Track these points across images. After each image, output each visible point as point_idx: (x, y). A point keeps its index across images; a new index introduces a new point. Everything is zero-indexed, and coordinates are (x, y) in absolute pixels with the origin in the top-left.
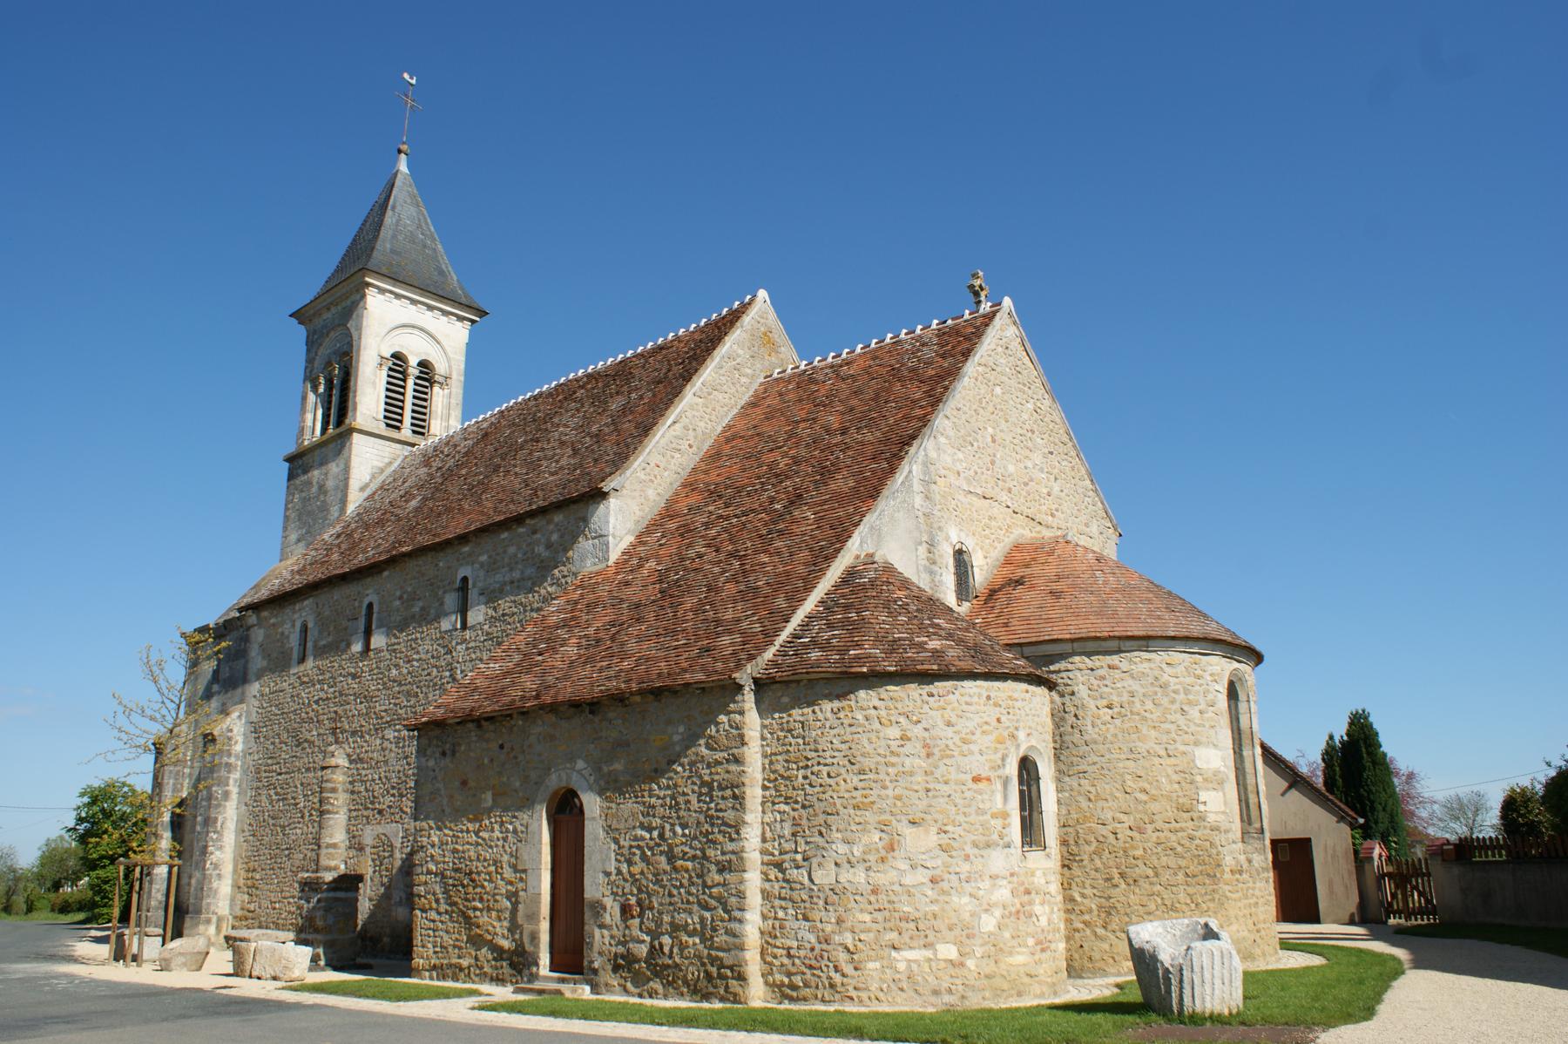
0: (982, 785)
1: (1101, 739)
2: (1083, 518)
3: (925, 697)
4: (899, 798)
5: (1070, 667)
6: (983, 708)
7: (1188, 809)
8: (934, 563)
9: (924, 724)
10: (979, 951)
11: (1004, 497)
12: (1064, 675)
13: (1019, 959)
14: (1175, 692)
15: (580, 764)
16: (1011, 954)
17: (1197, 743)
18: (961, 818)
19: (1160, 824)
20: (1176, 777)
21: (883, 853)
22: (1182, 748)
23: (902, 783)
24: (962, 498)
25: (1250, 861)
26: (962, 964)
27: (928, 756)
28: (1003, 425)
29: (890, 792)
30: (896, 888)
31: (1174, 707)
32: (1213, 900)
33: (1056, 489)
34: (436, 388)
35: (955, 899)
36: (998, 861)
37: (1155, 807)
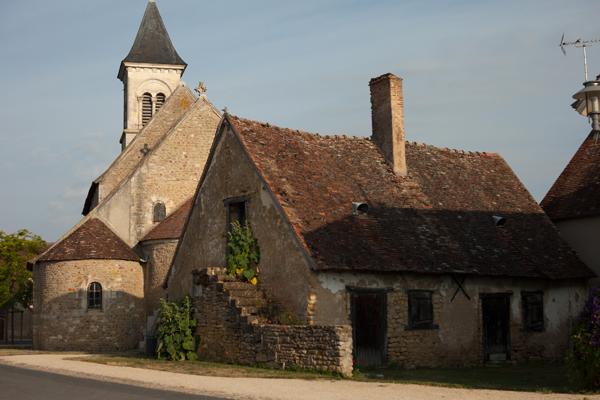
10: (68, 337)
13: (83, 340)
24: (164, 183)
28: (194, 149)
36: (76, 313)
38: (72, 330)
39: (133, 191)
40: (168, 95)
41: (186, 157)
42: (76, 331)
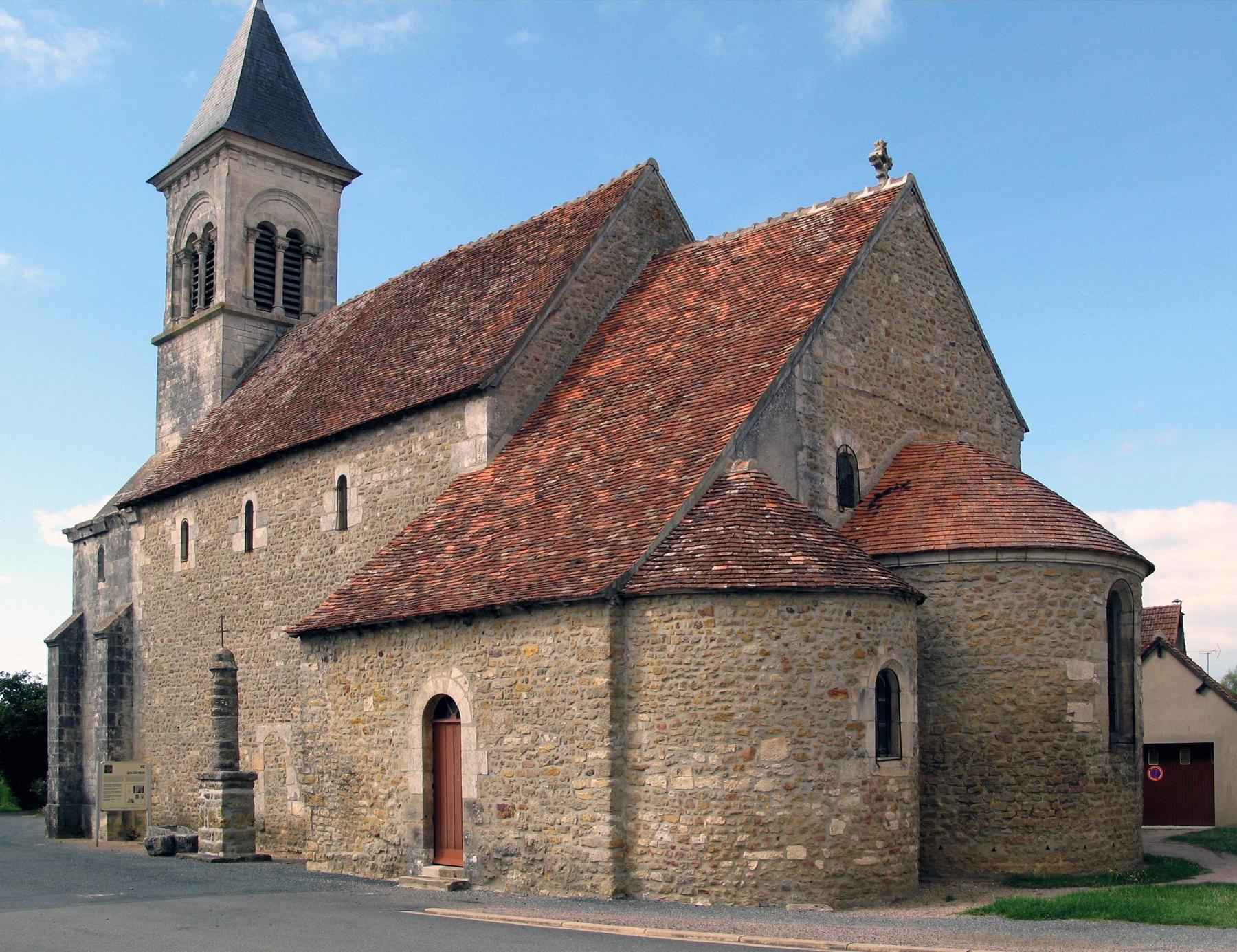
0: (838, 699)
1: (973, 651)
2: (985, 414)
3: (787, 614)
4: (757, 711)
5: (945, 577)
6: (842, 624)
7: (1057, 720)
8: (815, 468)
9: (784, 639)
11: (896, 395)
12: (938, 585)
13: (866, 860)
14: (1052, 604)
15: (456, 672)
16: (860, 856)
17: (1070, 656)
18: (816, 730)
19: (1025, 735)
20: (1043, 688)
21: (741, 762)
22: (1054, 660)
23: (762, 695)
24: (850, 399)
25: (1116, 770)
26: (813, 865)
27: (787, 670)
29: (748, 705)
30: (752, 794)
31: (1049, 620)
32: (1074, 807)
33: (957, 383)
34: (308, 262)
35: (807, 805)
36: (850, 770)
37: (1022, 718)
38: (838, 827)
39: (800, 404)
40: (311, 237)
41: (888, 334)
42: (850, 830)
